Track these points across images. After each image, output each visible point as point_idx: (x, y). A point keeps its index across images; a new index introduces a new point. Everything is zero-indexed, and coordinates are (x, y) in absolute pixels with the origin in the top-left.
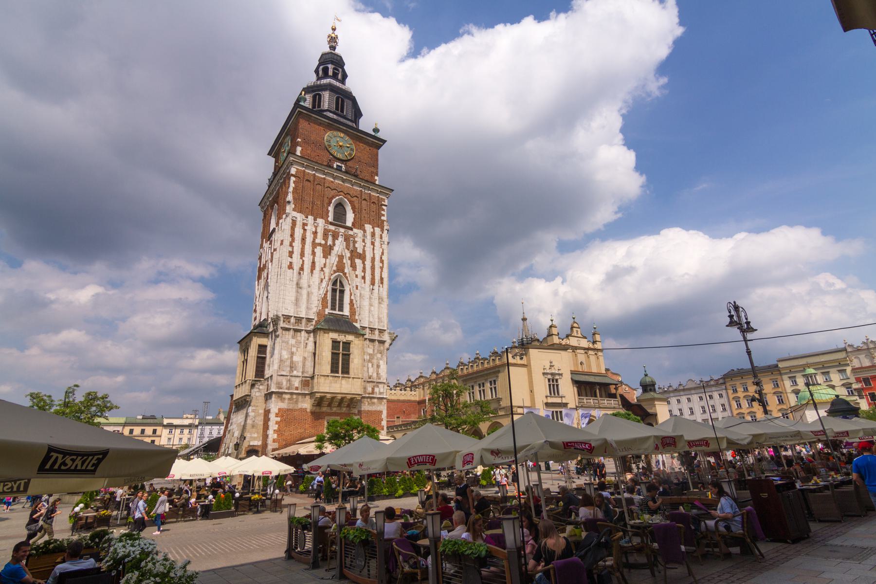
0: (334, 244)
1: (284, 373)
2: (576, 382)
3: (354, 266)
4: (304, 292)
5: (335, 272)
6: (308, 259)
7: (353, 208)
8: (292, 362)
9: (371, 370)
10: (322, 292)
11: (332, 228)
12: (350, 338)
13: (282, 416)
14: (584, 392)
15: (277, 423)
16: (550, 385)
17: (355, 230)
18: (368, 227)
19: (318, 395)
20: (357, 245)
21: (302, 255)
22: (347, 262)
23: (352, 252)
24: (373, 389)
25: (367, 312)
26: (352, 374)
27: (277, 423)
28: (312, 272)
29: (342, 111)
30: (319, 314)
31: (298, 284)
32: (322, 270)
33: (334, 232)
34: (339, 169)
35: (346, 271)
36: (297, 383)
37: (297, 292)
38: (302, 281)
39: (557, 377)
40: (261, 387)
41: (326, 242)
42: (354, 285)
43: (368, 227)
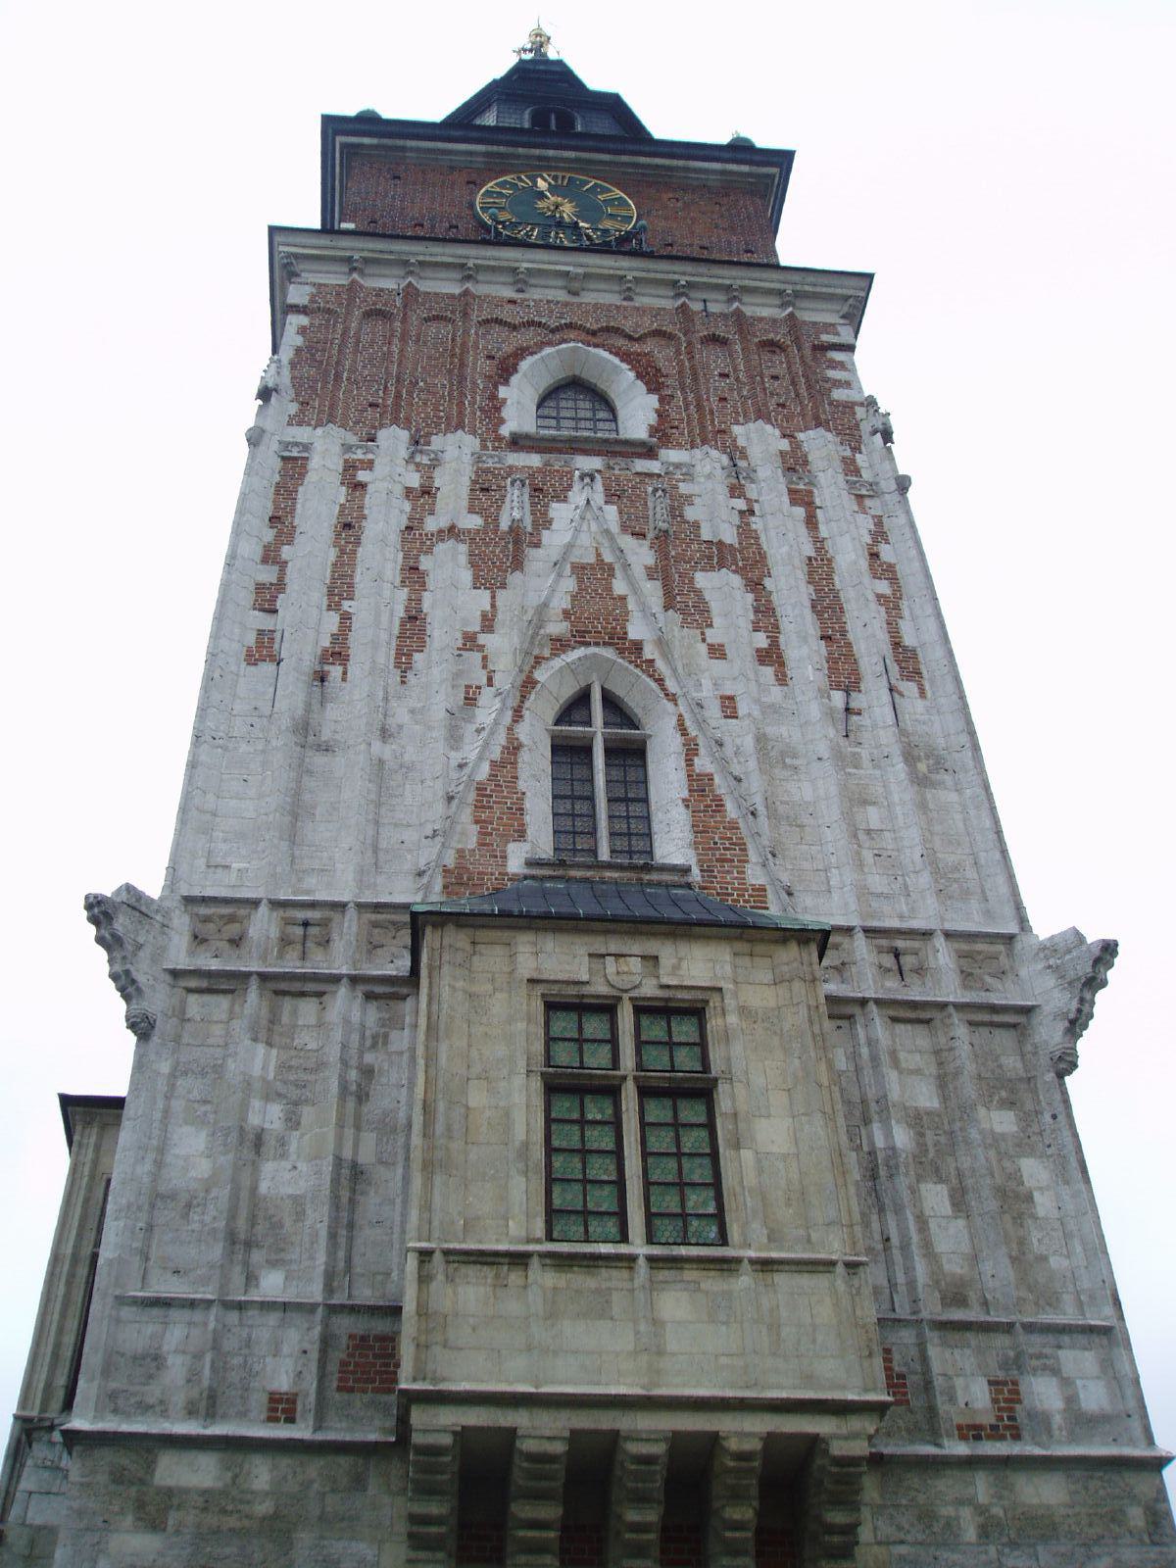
0: (543, 522)
5: (560, 645)
6: (377, 604)
9: (951, 1238)
10: (477, 753)
12: (694, 965)
17: (673, 455)
18: (761, 440)
21: (340, 589)
24: (1006, 1392)
26: (748, 1240)
28: (403, 660)
32: (470, 642)
35: (636, 630)
37: (302, 770)
38: (332, 712)
41: (492, 520)
42: (707, 692)
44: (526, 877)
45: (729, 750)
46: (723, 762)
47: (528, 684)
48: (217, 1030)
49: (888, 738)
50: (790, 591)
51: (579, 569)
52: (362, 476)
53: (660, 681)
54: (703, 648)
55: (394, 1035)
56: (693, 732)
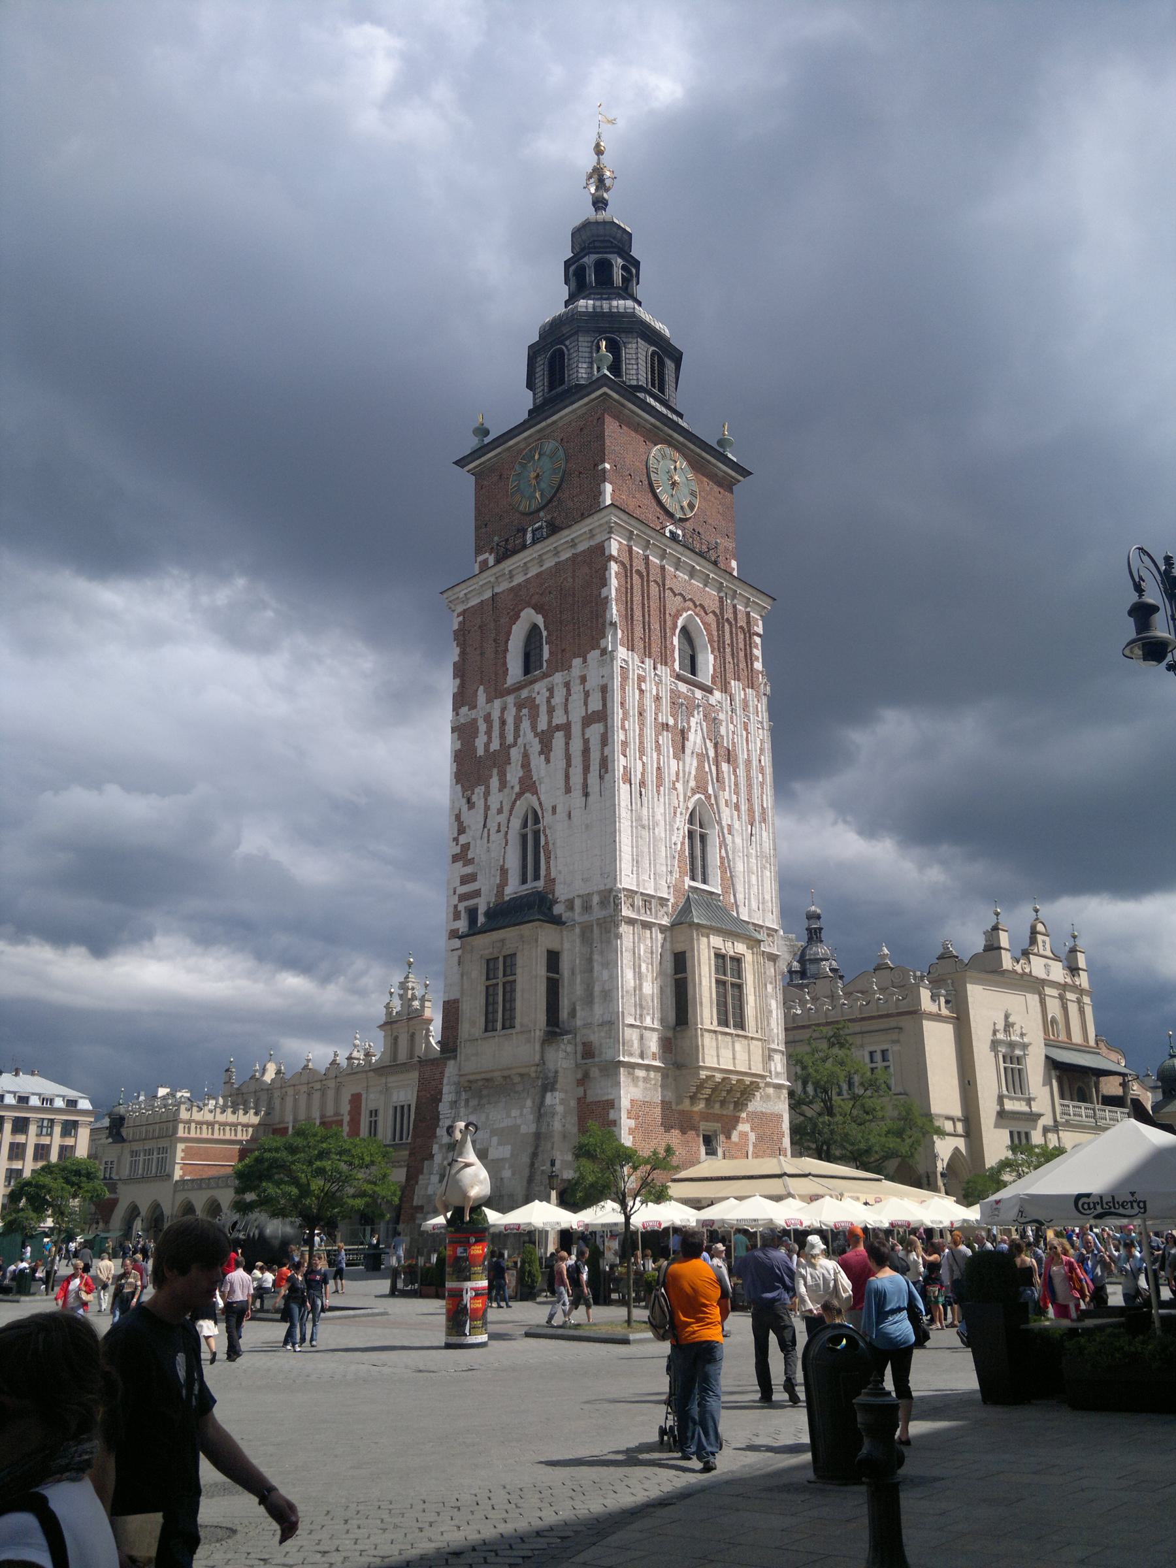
0: (689, 727)
2: (1053, 1065)
5: (694, 792)
6: (651, 758)
11: (683, 687)
12: (741, 948)
14: (1067, 1093)
15: (631, 1131)
16: (1005, 1068)
17: (717, 694)
19: (703, 1074)
21: (642, 752)
23: (716, 746)
27: (631, 1131)
30: (677, 889)
35: (710, 791)
39: (1018, 1052)
41: (676, 723)
50: (741, 772)
51: (698, 755)
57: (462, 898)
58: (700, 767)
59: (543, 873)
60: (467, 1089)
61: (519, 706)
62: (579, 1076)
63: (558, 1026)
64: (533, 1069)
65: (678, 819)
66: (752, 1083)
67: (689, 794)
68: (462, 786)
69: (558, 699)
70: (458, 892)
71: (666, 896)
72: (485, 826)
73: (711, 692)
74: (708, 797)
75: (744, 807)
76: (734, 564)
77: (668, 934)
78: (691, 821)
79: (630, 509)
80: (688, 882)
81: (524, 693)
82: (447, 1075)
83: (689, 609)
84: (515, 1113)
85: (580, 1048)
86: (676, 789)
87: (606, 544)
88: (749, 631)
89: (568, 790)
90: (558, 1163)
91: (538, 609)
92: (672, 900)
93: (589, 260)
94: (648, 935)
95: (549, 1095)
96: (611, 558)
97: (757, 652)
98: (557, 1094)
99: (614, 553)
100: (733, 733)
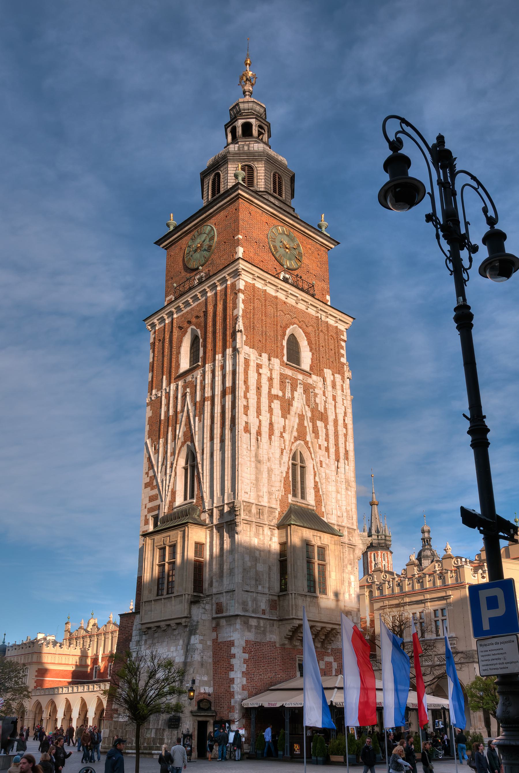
0: (293, 398)
1: (248, 588)
3: (315, 431)
4: (264, 468)
5: (296, 439)
7: (310, 343)
8: (257, 573)
10: (284, 469)
11: (289, 372)
12: (325, 539)
13: (250, 652)
15: (245, 661)
17: (314, 377)
18: (328, 373)
20: (318, 400)
21: (259, 412)
22: (308, 424)
23: (312, 411)
25: (334, 501)
27: (245, 661)
28: (270, 438)
29: (280, 194)
30: (283, 501)
31: (256, 456)
32: (282, 436)
33: (292, 378)
34: (285, 280)
35: (308, 438)
36: (263, 605)
37: (256, 468)
38: (260, 451)
40: (208, 607)
42: (318, 460)
43: (328, 373)
44: (291, 504)
45: (321, 476)
46: (320, 479)
47: (291, 450)
48: (248, 533)
49: (343, 476)
50: (331, 427)
51: (299, 415)
52: (261, 371)
53: (311, 453)
54: (318, 445)
55: (273, 538)
56: (316, 470)
57: (150, 510)
58: (301, 424)
59: (196, 492)
60: (145, 633)
61: (185, 387)
62: (214, 625)
63: (202, 593)
64: (184, 620)
65: (284, 457)
66: (333, 629)
67: (292, 440)
68: (152, 440)
69: (208, 380)
70: (147, 507)
71: (274, 506)
72: (163, 465)
73: (311, 377)
74: (306, 443)
75: (332, 450)
76: (328, 298)
77: (276, 532)
78: (294, 458)
79: (256, 262)
80: (290, 498)
81: (189, 378)
82: (135, 623)
83: (294, 324)
84: (173, 649)
85: (214, 607)
86: (283, 437)
87: (237, 283)
88: (337, 337)
89: (212, 439)
90: (197, 682)
91: (198, 325)
92: (279, 510)
93: (240, 122)
94: (261, 532)
95: (193, 637)
96: (239, 290)
97: (343, 352)
98: (197, 636)
99: (242, 287)
100: (325, 402)
